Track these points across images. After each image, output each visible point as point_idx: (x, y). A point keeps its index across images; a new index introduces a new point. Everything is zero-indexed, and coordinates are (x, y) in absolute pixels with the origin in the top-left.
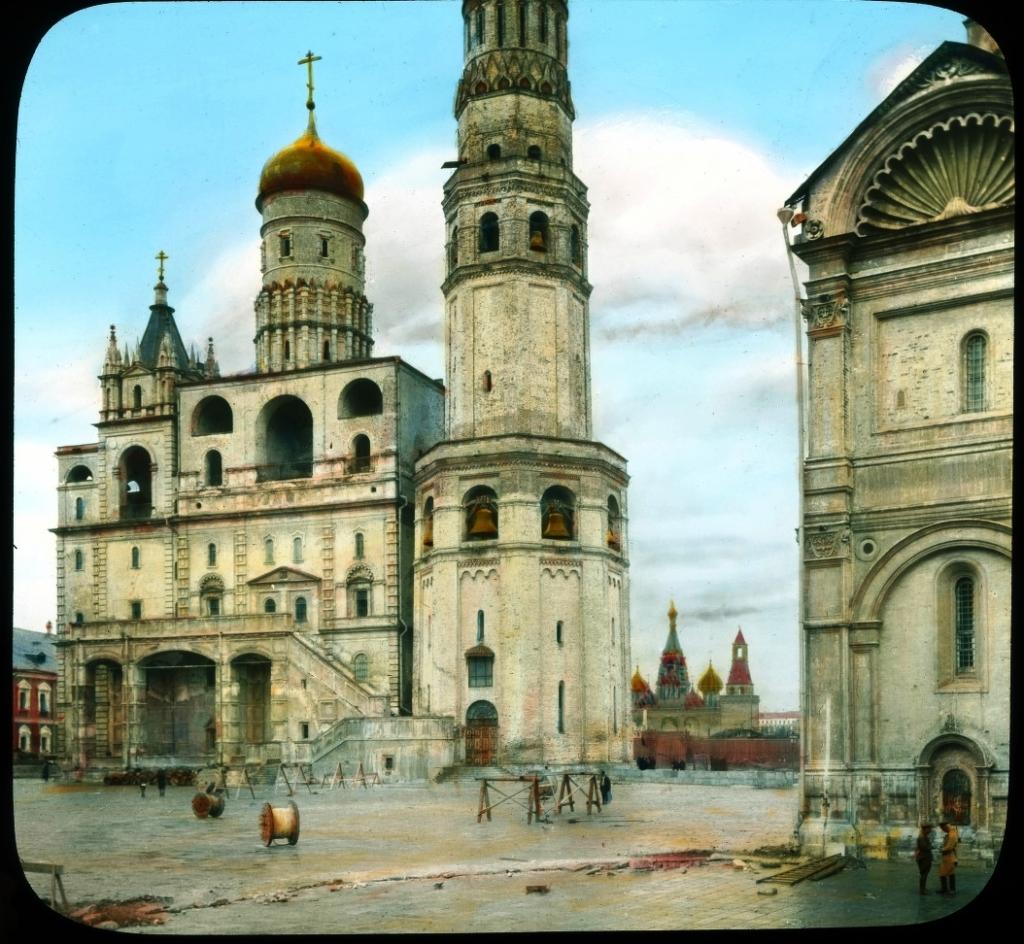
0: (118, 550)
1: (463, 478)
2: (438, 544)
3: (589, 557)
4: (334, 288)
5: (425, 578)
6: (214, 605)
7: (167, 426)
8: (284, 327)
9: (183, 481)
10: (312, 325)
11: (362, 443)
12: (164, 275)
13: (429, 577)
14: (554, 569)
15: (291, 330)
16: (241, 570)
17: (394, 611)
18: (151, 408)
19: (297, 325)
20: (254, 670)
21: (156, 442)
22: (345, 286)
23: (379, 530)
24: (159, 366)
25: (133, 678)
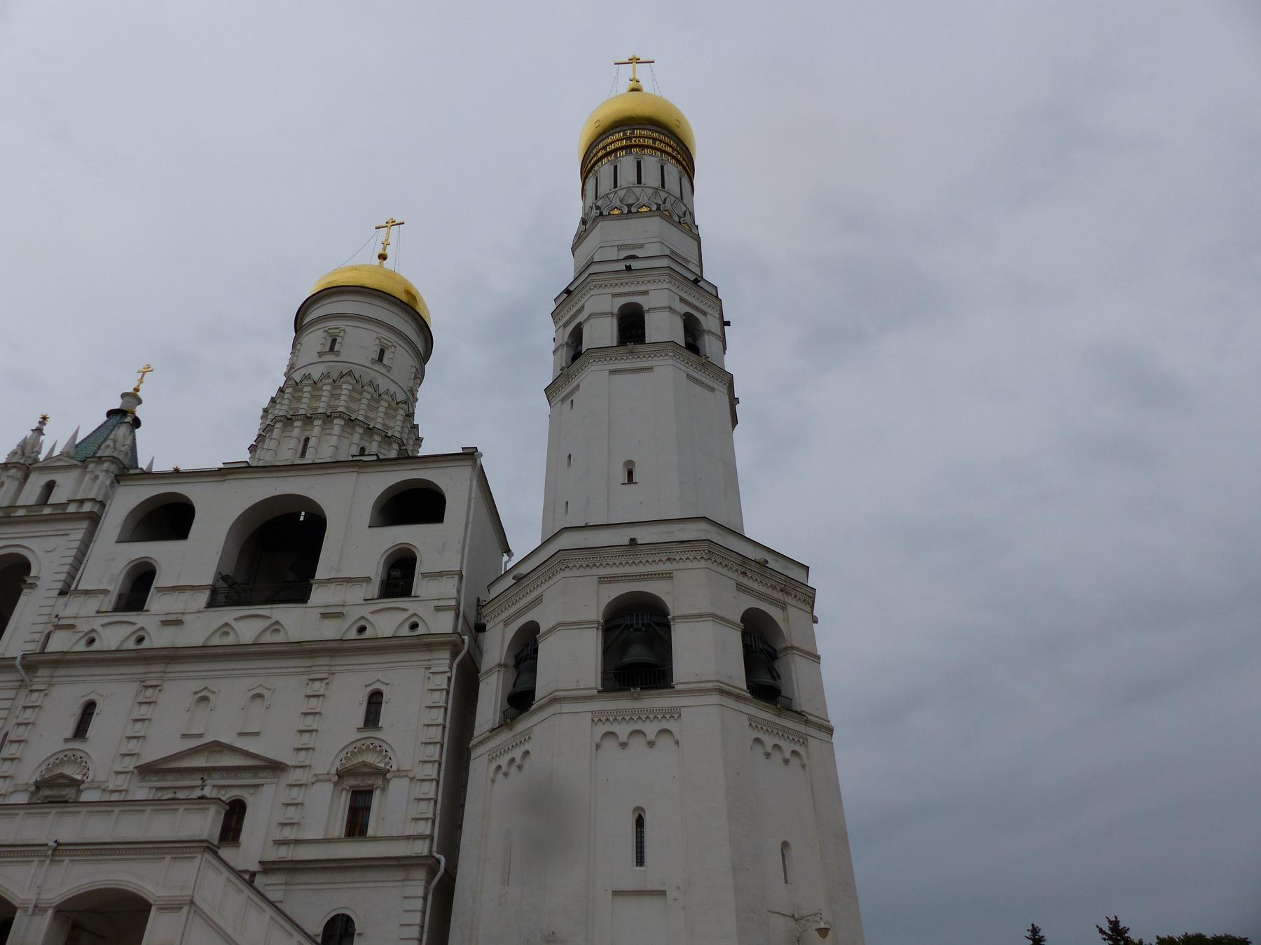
1: (603, 580)
3: (812, 731)
4: (387, 392)
5: (503, 761)
7: (77, 532)
8: (308, 420)
10: (351, 422)
12: (141, 387)
13: (517, 754)
14: (769, 741)
15: (318, 422)
16: (133, 746)
17: (424, 828)
18: (64, 505)
19: (328, 418)
24: (99, 455)
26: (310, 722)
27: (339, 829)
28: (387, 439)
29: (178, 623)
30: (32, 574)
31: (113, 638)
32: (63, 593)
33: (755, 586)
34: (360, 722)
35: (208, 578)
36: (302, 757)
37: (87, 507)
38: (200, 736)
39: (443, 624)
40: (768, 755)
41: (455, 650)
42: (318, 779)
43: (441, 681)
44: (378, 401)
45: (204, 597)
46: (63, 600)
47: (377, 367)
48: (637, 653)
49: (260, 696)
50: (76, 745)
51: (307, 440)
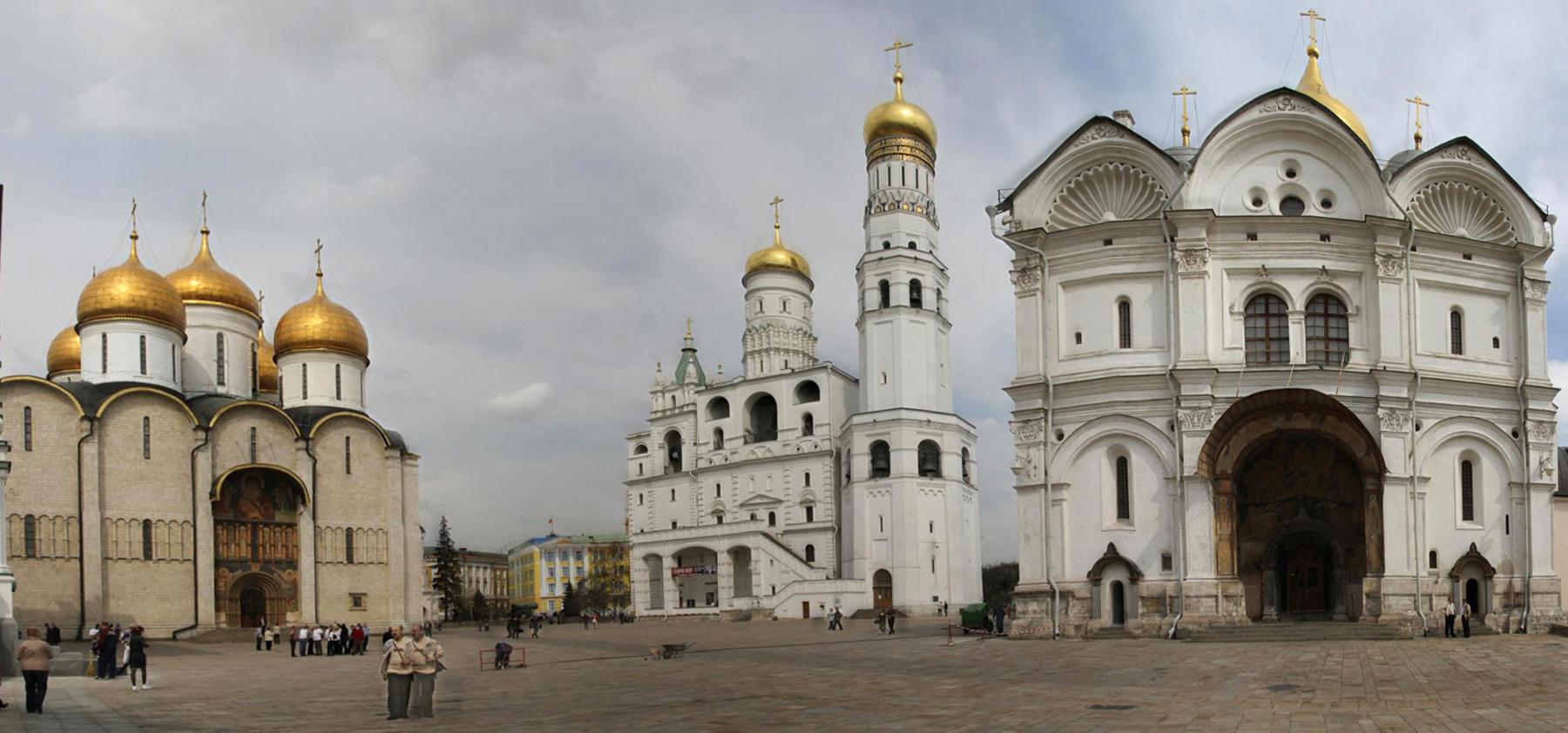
0: (662, 490)
1: (871, 435)
2: (855, 475)
4: (791, 328)
6: (720, 520)
9: (699, 448)
10: (777, 350)
11: (808, 419)
14: (927, 489)
16: (735, 498)
17: (830, 518)
18: (682, 407)
20: (741, 555)
21: (684, 427)
22: (798, 328)
23: (822, 471)
25: (669, 563)
26: (786, 486)
27: (805, 520)
28: (796, 352)
29: (736, 453)
30: (683, 437)
31: (718, 460)
32: (695, 444)
33: (927, 430)
34: (804, 485)
35: (741, 433)
36: (787, 498)
37: (691, 408)
38: (754, 492)
39: (826, 446)
40: (926, 494)
41: (831, 455)
42: (795, 505)
43: (828, 468)
44: (788, 333)
45: (742, 440)
46: (695, 448)
47: (784, 314)
48: (881, 464)
49: (769, 477)
50: (719, 499)
51: (762, 362)
